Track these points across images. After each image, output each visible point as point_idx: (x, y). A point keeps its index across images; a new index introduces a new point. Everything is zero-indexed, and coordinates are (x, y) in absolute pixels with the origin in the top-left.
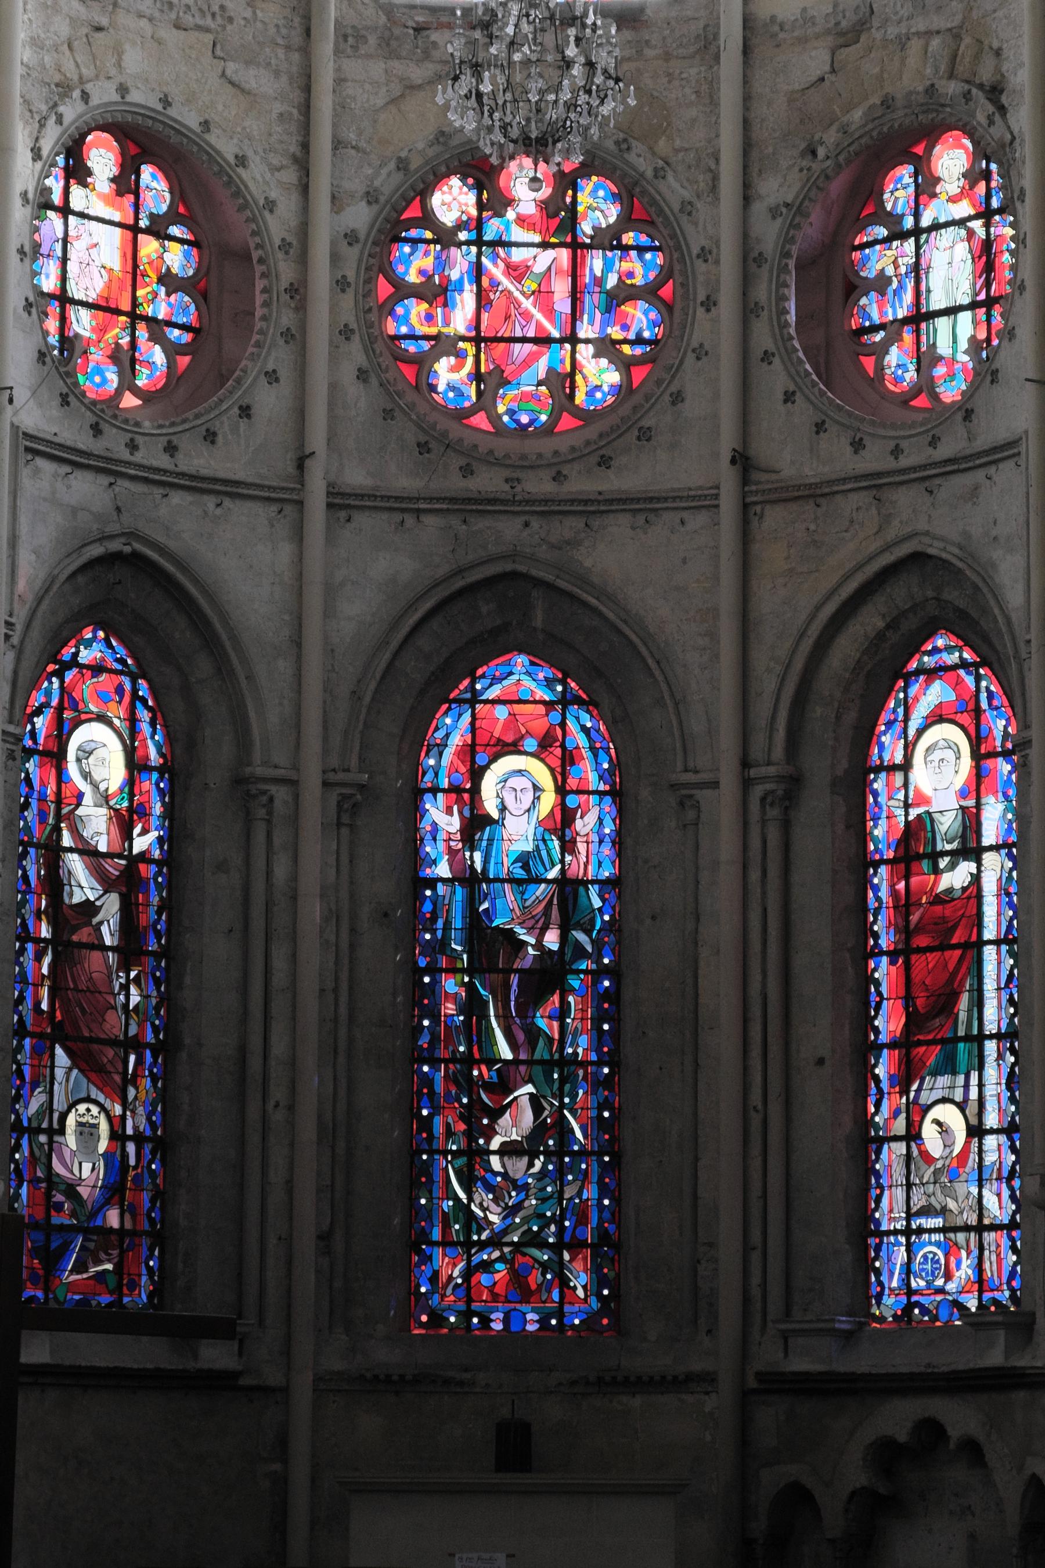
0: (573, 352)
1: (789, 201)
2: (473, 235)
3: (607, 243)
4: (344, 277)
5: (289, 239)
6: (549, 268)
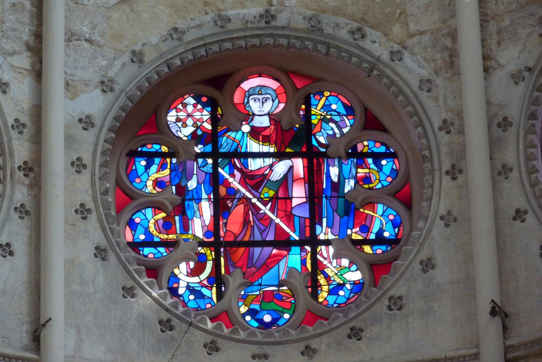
0: (314, 254)
1: (531, 64)
2: (209, 148)
3: (342, 153)
4: (79, 159)
5: (25, 119)
6: (285, 177)
